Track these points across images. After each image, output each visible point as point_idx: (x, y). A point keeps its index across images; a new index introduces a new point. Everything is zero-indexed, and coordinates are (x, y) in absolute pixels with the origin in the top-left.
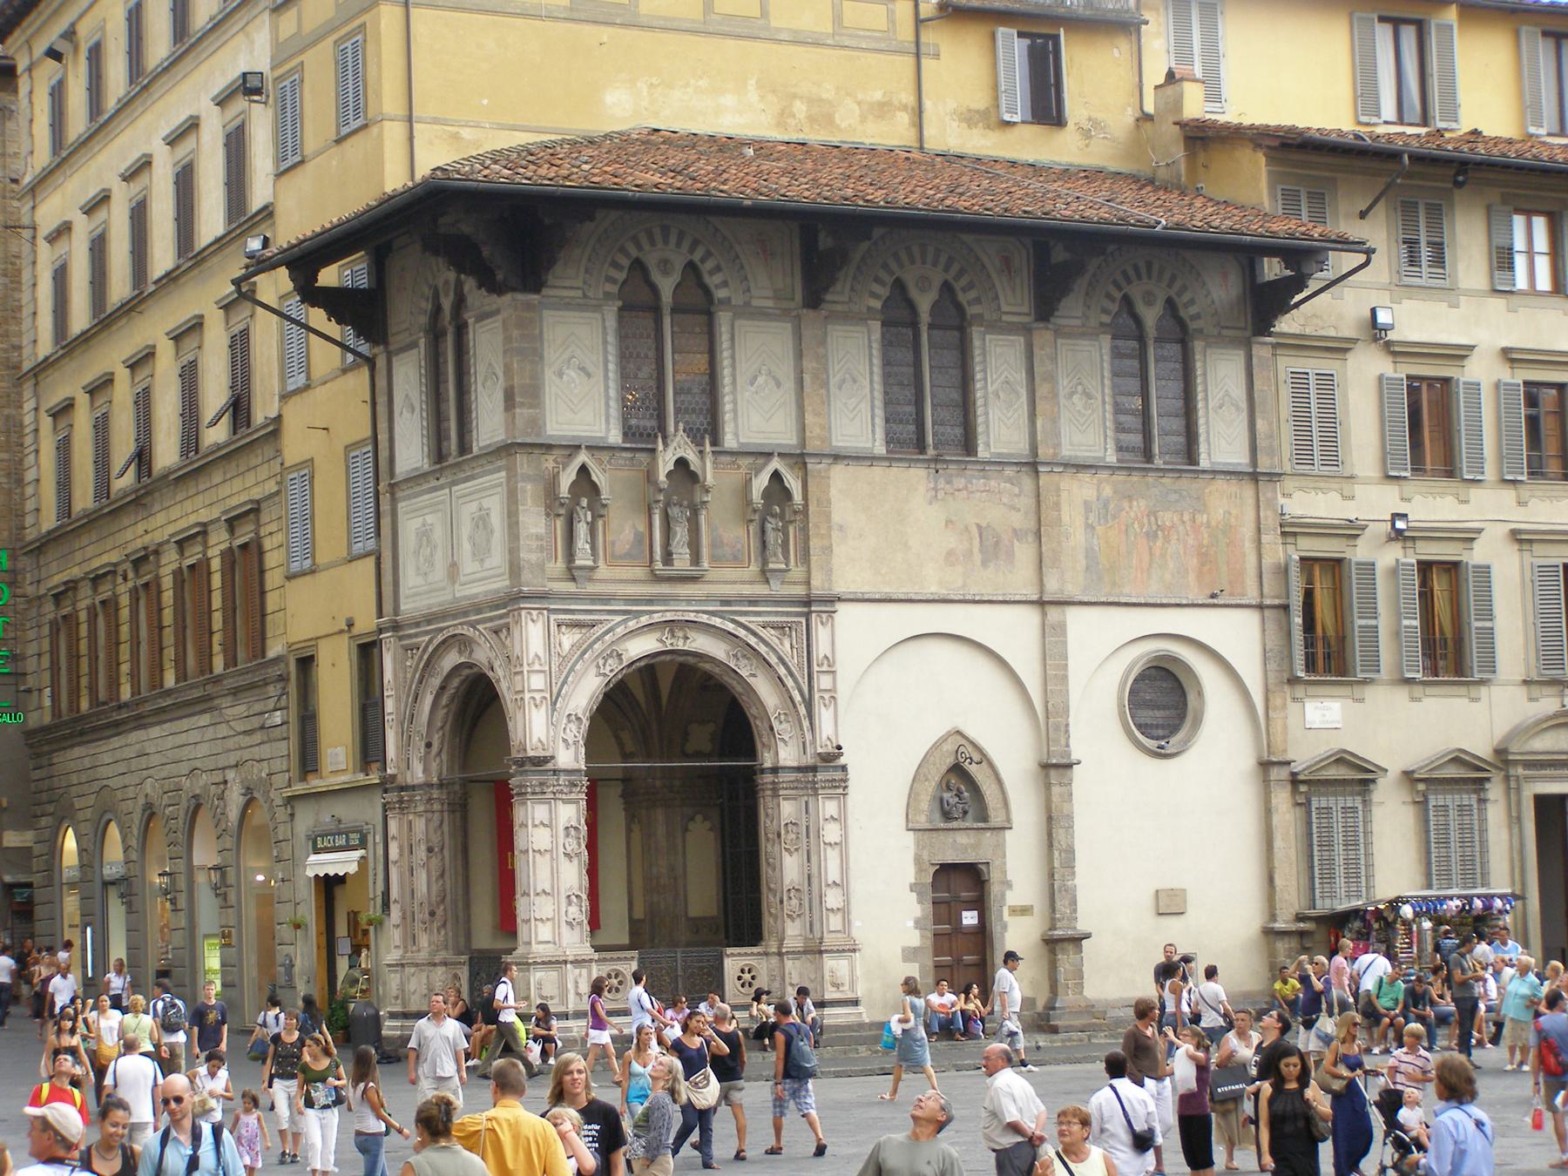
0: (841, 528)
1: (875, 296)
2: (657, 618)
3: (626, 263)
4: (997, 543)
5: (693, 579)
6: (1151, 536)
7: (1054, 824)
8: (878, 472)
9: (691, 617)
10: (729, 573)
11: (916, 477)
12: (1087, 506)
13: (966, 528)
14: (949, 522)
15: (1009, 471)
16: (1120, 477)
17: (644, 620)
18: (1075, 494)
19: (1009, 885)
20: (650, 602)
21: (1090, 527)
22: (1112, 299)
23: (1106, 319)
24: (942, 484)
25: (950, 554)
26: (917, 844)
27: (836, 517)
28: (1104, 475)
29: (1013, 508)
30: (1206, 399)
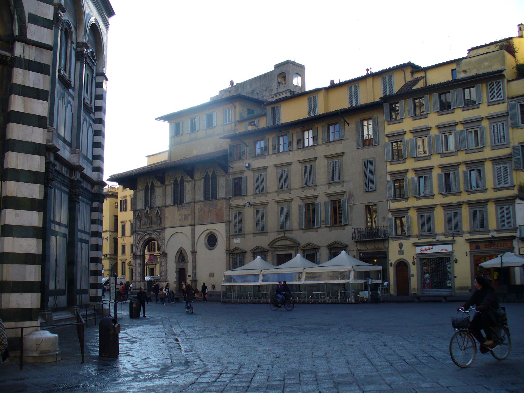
0: (167, 217)
1: (172, 181)
2: (147, 233)
3: (146, 183)
4: (186, 217)
5: (151, 227)
6: (208, 212)
7: (194, 261)
8: (172, 208)
9: (150, 233)
10: (154, 226)
11: (176, 208)
12: (199, 208)
13: (182, 215)
14: (180, 214)
15: (188, 205)
16: (204, 203)
17: (146, 233)
18: (198, 206)
19: (188, 272)
20: (146, 231)
21: (199, 212)
22: (204, 173)
23: (203, 176)
24: (179, 208)
25: (180, 219)
26: (176, 266)
27: (166, 216)
28: (201, 203)
29: (188, 211)
30: (218, 187)
